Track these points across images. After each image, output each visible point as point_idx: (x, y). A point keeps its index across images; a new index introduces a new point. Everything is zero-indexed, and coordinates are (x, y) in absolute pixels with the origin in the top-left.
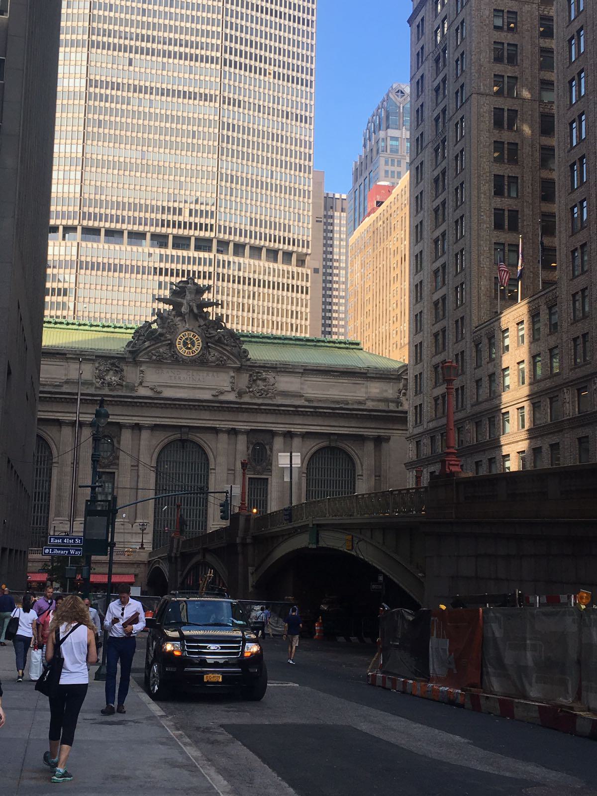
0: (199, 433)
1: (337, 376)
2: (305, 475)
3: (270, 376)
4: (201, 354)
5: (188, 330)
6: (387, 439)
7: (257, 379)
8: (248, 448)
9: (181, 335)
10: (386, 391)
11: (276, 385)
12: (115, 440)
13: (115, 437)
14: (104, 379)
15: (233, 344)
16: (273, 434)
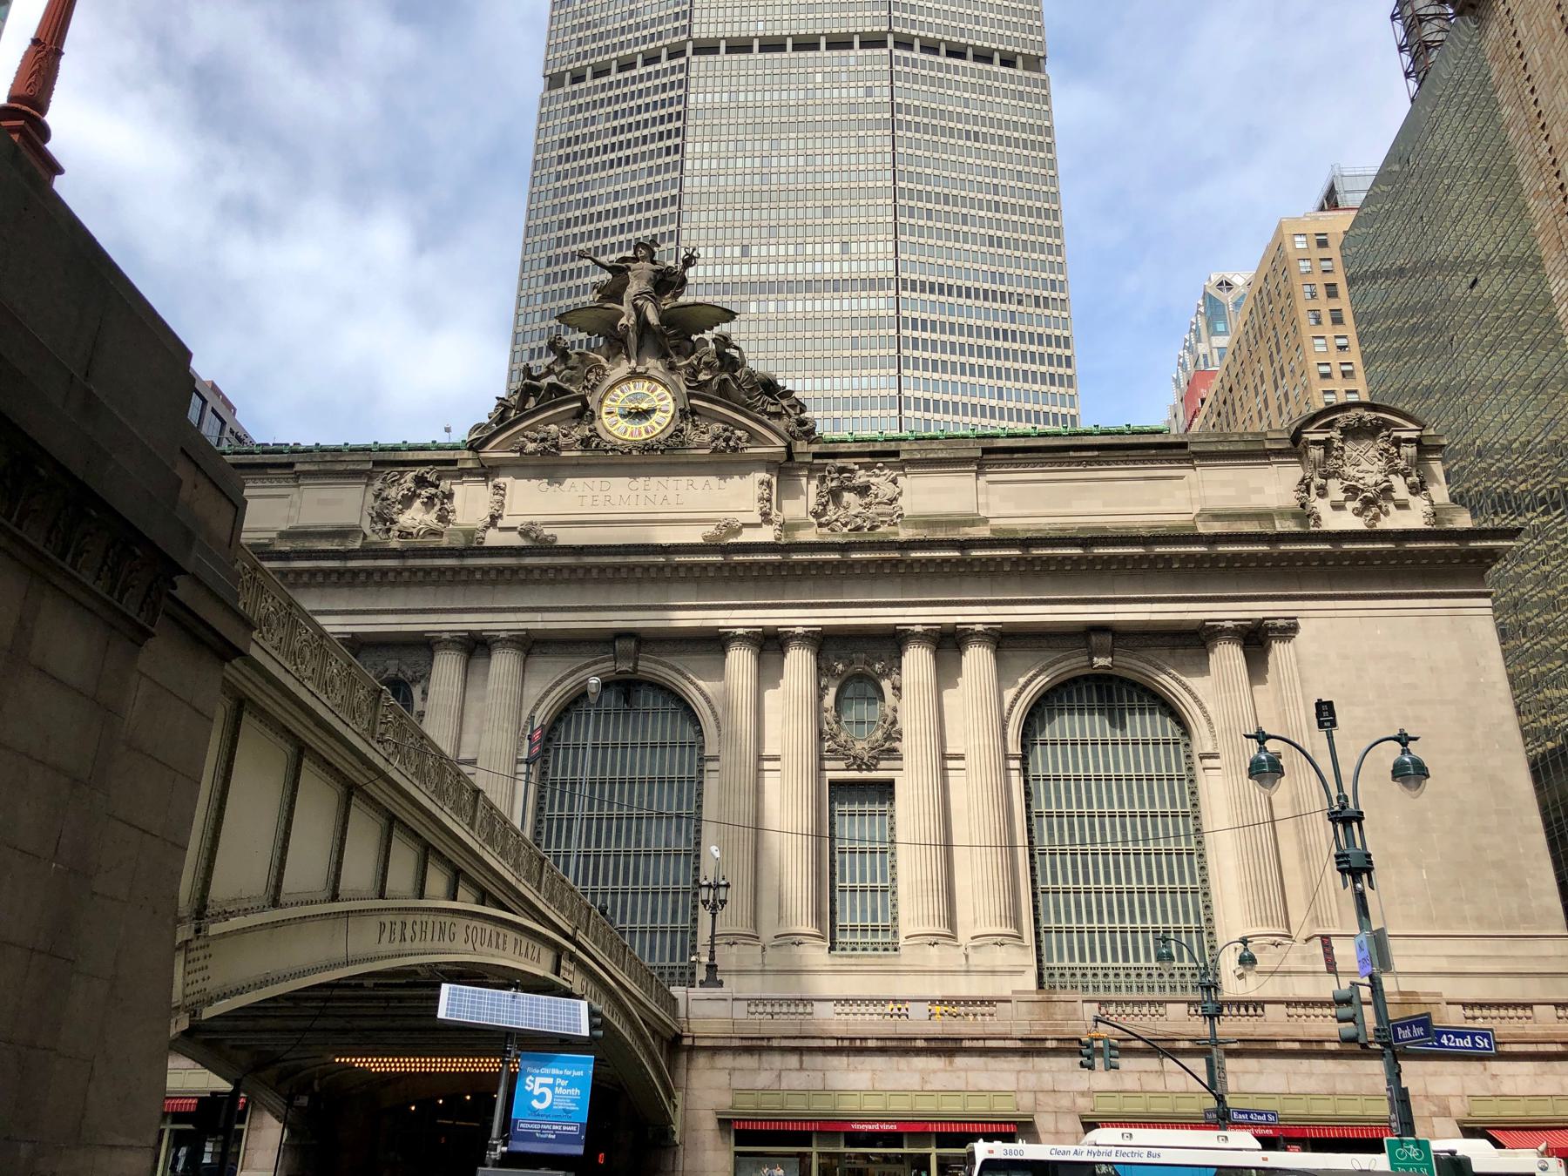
0: (671, 654)
1: (1089, 463)
2: (1015, 764)
3: (881, 482)
4: (670, 430)
5: (634, 375)
6: (1289, 631)
7: (842, 488)
8: (821, 692)
9: (618, 391)
10: (1260, 491)
11: (901, 501)
12: (417, 692)
13: (415, 681)
14: (393, 522)
15: (772, 409)
16: (893, 641)
